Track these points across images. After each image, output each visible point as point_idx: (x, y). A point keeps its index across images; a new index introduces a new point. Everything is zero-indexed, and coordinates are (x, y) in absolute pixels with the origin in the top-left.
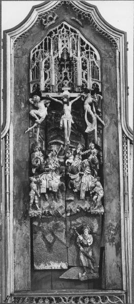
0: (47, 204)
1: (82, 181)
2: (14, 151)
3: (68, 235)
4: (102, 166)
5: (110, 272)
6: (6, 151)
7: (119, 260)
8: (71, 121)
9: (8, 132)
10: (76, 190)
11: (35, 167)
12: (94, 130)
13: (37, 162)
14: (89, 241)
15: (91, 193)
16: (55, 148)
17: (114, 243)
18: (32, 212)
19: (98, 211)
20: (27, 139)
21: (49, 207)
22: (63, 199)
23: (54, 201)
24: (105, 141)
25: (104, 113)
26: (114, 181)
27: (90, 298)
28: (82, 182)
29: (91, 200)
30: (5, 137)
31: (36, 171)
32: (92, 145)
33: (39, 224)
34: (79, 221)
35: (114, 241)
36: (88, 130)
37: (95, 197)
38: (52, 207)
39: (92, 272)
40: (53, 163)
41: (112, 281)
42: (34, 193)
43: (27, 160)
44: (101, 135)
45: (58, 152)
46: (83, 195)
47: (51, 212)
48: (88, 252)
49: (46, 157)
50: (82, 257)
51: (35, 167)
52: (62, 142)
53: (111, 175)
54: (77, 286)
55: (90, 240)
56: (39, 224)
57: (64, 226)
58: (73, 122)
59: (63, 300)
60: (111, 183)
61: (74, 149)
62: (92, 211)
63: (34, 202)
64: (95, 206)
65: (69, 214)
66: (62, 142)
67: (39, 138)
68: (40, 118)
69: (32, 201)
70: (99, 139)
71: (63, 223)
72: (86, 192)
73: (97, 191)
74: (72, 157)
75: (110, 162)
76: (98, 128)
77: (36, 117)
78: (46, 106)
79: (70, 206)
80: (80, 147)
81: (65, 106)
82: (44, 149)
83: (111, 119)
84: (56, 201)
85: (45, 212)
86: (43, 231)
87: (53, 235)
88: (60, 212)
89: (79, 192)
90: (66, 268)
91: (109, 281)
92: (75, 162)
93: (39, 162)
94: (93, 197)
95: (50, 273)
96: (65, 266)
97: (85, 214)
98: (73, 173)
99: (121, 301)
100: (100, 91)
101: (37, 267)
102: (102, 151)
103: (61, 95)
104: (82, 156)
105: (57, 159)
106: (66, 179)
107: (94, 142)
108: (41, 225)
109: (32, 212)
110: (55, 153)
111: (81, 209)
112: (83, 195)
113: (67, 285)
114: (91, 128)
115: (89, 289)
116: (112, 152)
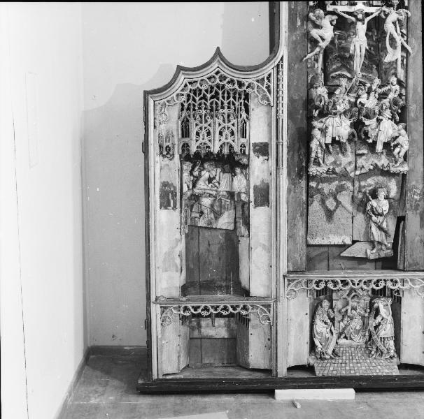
2: (289, 86)
3: (356, 200)
4: (404, 108)
6: (278, 85)
8: (365, 46)
9: (282, 59)
11: (317, 108)
13: (321, 101)
14: (384, 209)
15: (392, 144)
17: (418, 212)
18: (313, 170)
19: (402, 169)
21: (335, 163)
22: (352, 152)
23: (340, 155)
24: (411, 74)
25: (410, 36)
30: (278, 65)
32: (393, 80)
33: (318, 185)
34: (371, 182)
35: (418, 209)
36: (388, 59)
37: (397, 150)
38: (338, 163)
39: (384, 247)
41: (413, 260)
42: (318, 143)
43: (304, 99)
45: (348, 89)
47: (337, 170)
48: (382, 223)
49: (331, 94)
50: (374, 229)
51: (317, 108)
52: (349, 75)
53: (417, 120)
54: (360, 266)
55: (383, 205)
56: (318, 185)
57: (351, 188)
58: (367, 48)
60: (416, 131)
61: (368, 85)
62: (392, 170)
64: (396, 162)
66: (349, 75)
68: (323, 39)
70: (403, 71)
71: (349, 184)
72: (384, 143)
73: (400, 143)
74: (366, 95)
77: (320, 39)
78: (332, 24)
79: (361, 161)
80: (377, 81)
81: (359, 24)
84: (343, 153)
85: (329, 169)
86: (323, 194)
87: (335, 199)
89: (375, 143)
90: (351, 243)
91: (409, 260)
92: (370, 102)
93: (323, 102)
95: (326, 249)
96: (348, 242)
97: (379, 172)
98: (367, 116)
100: (406, 4)
101: (311, 242)
103: (352, 9)
105: (347, 98)
106: (358, 125)
107: (396, 76)
108: (320, 187)
112: (379, 147)
113: (349, 264)
114: (392, 55)
115: (376, 269)
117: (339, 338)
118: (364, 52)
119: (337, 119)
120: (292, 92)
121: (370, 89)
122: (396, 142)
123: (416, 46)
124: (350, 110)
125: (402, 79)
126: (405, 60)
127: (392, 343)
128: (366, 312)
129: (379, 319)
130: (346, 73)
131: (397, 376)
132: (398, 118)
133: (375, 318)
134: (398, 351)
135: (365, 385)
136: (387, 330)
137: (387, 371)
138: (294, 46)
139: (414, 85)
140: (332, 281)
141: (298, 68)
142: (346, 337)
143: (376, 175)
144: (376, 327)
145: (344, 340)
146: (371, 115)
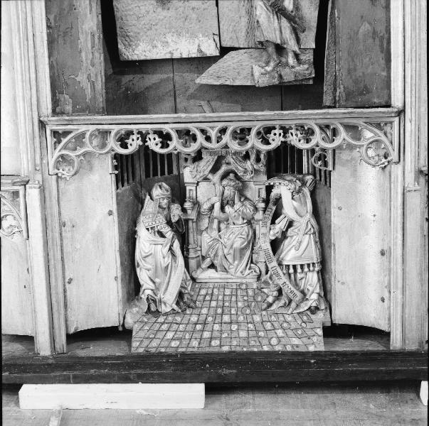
5: (349, 53)
7: (380, 13)
27: (285, 130)
59: (200, 138)
96: (212, 51)
99: (383, 138)
117: (199, 266)
127: (313, 278)
128: (256, 209)
129: (281, 224)
131: (316, 354)
133: (273, 222)
134: (326, 293)
135: (229, 375)
136: (299, 249)
137: (296, 341)
140: (155, 132)
142: (212, 266)
144: (276, 245)
145: (211, 272)
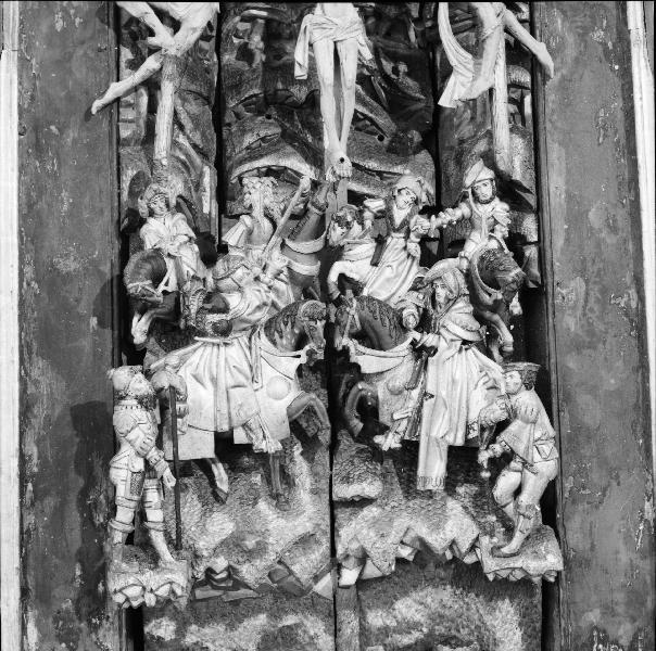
0: (221, 525)
1: (430, 389)
4: (534, 296)
10: (388, 442)
12: (491, 91)
13: (157, 277)
15: (484, 457)
16: (259, 193)
18: (129, 584)
20: (106, 151)
21: (233, 544)
22: (315, 492)
23: (262, 505)
24: (554, 154)
26: (612, 383)
28: (425, 395)
29: (484, 502)
31: (149, 333)
32: (478, 176)
33: (181, 631)
36: (452, 95)
37: (507, 481)
40: (257, 279)
42: (139, 465)
44: (531, 128)
46: (433, 468)
47: (250, 572)
49: (212, 251)
56: (181, 631)
60: (593, 390)
61: (375, 205)
63: (141, 515)
64: (510, 531)
65: (349, 576)
67: (175, 144)
68: (175, 25)
69: (125, 515)
70: (519, 142)
71: (315, 627)
73: (520, 449)
74: (368, 248)
75: (582, 272)
76: (512, 85)
79: (356, 531)
82: (209, 206)
83: (583, 34)
85: (210, 571)
88: (304, 566)
89: (410, 449)
92: (388, 278)
93: (171, 276)
94: (493, 481)
102: (538, 211)
104: (424, 240)
105: (278, 261)
106: (331, 373)
107: (489, 159)
108: (190, 639)
109: (129, 584)
110: (267, 224)
111: (424, 551)
112: (433, 468)
116: (594, 217)
118: (350, 71)
119: (234, 352)
120: (53, 239)
121: (384, 215)
122: (498, 449)
123: (570, 39)
124: (290, 311)
125: (519, 172)
126: (528, 100)
130: (295, 163)
132: (507, 337)
138: (57, 53)
139: (570, 197)
141: (75, 141)
143: (433, 582)
146: (385, 329)
